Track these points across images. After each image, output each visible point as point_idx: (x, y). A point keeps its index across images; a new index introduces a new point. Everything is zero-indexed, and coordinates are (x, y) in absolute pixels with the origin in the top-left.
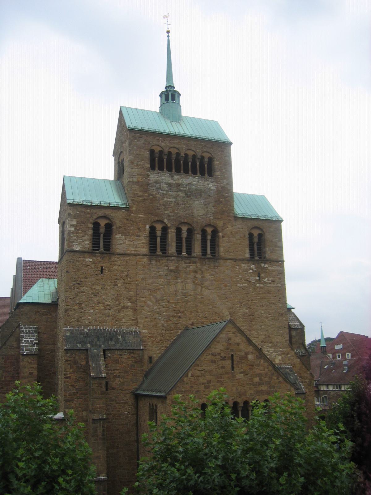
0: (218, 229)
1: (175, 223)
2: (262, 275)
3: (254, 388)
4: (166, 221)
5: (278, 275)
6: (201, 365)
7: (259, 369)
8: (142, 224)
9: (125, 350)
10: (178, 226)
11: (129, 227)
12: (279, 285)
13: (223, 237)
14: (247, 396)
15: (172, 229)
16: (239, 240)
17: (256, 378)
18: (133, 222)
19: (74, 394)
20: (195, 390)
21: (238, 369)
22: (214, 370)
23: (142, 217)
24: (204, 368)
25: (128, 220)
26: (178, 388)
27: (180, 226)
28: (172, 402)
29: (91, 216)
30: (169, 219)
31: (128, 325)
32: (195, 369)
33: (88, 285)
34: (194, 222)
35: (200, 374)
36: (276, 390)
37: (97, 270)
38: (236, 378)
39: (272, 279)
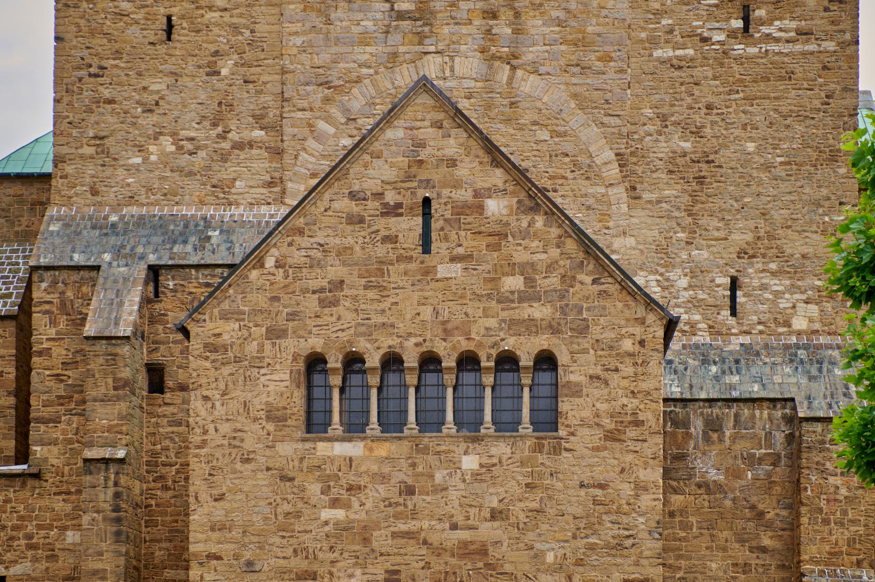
2: (760, 13)
3: (502, 309)
5: (826, 9)
6: (310, 230)
7: (525, 248)
9: (220, 270)
12: (830, 46)
14: (472, 336)
17: (511, 278)
19: (61, 401)
20: (286, 310)
26: (227, 301)
28: (206, 346)
31: (253, 201)
33: (125, 78)
35: (308, 260)
36: (584, 320)
37: (153, 27)
38: (436, 274)
39: (803, 23)
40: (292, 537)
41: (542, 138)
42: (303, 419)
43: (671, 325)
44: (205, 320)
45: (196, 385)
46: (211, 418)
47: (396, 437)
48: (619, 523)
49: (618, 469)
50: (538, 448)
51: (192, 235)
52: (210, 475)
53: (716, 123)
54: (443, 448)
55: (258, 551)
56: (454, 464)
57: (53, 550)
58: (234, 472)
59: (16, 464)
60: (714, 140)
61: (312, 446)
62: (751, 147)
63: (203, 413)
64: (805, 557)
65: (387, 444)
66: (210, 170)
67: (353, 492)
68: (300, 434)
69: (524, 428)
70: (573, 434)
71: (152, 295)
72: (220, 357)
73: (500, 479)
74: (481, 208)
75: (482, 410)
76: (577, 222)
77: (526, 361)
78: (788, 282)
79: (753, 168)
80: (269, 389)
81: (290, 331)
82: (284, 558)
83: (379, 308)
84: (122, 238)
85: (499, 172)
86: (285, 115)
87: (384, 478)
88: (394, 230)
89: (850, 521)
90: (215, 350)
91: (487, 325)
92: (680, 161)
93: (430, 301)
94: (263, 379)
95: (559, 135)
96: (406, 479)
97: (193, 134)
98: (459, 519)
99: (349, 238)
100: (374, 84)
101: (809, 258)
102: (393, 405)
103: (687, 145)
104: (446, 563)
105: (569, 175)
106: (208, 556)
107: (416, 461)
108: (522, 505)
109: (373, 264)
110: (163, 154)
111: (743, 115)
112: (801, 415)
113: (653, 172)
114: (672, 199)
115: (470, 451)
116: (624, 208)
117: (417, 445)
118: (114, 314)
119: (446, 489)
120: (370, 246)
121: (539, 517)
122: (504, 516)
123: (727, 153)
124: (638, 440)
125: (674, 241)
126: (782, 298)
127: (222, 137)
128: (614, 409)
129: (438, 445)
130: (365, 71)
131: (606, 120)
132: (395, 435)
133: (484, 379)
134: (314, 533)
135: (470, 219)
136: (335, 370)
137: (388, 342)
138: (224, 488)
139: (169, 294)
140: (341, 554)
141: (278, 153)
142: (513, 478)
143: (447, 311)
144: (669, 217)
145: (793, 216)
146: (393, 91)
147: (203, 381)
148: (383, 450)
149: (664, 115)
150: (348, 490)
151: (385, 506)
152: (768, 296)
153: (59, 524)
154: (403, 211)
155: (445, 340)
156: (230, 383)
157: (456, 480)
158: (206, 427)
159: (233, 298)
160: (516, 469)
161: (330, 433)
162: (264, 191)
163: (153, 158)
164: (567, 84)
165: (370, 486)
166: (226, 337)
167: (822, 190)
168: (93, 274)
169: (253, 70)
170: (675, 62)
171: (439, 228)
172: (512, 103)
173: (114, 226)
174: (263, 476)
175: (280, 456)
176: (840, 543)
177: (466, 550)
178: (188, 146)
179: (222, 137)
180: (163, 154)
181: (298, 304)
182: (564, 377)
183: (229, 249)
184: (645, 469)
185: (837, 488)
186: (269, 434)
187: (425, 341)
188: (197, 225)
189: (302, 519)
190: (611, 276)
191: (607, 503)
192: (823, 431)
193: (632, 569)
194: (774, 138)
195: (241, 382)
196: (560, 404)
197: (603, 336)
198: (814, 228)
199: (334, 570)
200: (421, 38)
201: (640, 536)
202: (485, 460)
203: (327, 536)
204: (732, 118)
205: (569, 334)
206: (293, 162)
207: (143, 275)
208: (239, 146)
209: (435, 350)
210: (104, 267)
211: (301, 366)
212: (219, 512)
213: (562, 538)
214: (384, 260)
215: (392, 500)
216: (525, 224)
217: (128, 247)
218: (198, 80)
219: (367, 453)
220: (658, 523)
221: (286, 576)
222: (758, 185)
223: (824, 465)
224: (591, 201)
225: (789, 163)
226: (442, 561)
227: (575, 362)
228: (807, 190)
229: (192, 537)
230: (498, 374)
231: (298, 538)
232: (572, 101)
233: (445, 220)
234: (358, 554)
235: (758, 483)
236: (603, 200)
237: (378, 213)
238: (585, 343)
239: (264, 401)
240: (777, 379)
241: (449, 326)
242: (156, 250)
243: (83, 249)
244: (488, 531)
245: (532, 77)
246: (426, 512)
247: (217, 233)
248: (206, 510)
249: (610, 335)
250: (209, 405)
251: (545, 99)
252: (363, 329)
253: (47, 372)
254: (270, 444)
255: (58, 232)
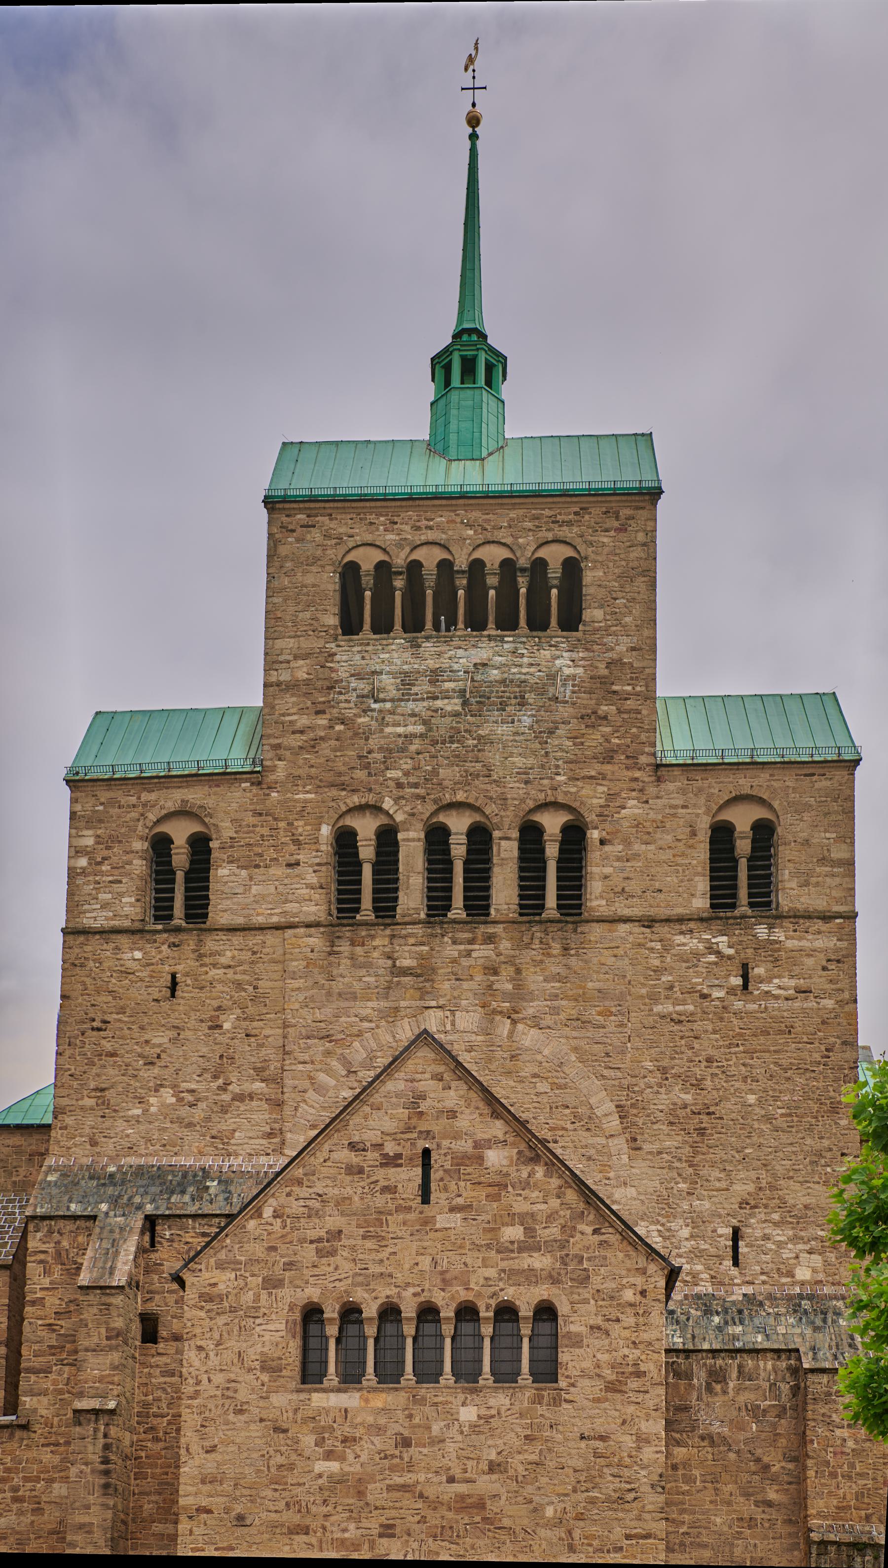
0: (586, 815)
1: (419, 807)
3: (502, 1259)
4: (388, 804)
7: (525, 1198)
8: (306, 825)
9: (217, 1220)
10: (435, 820)
11: (262, 836)
13: (602, 842)
15: (408, 830)
16: (670, 847)
18: (275, 819)
19: (53, 1351)
20: (283, 1260)
21: (444, 1195)
22: (356, 1198)
23: (306, 801)
24: (321, 1192)
25: (260, 814)
26: (224, 1250)
27: (442, 818)
29: (142, 815)
30: (403, 797)
32: (288, 1195)
34: (491, 798)
35: (306, 1210)
36: (585, 1270)
38: (435, 1224)
40: (284, 1490)
41: (542, 1090)
42: (298, 1369)
43: (673, 1275)
44: (200, 1270)
45: (190, 1335)
46: (204, 1369)
47: (392, 1388)
48: (620, 1477)
49: (619, 1421)
50: (538, 1400)
51: (190, 1185)
52: (202, 1426)
53: (717, 1075)
54: (440, 1399)
55: (249, 1505)
56: (452, 1415)
57: (39, 1503)
58: (227, 1423)
59: (4, 1415)
60: (714, 1092)
61: (308, 1397)
62: (752, 1099)
63: (197, 1363)
64: (812, 1511)
65: (384, 1395)
66: (210, 1121)
67: (348, 1444)
68: (293, 1385)
69: (523, 1379)
70: (573, 1385)
71: (147, 1245)
72: (215, 1307)
73: (499, 1430)
74: (480, 1159)
75: (481, 1361)
76: (578, 1173)
77: (526, 1311)
78: (791, 1233)
79: (754, 1120)
80: (264, 1339)
81: (286, 1281)
82: (276, 1511)
83: (377, 1258)
84: (119, 1188)
85: (499, 1123)
86: (286, 1068)
87: (379, 1430)
88: (393, 1180)
89: (857, 1474)
90: (211, 1300)
91: (487, 1275)
92: (681, 1113)
93: (429, 1251)
94: (258, 1329)
95: (559, 1087)
96: (402, 1430)
97: (193, 1086)
98: (457, 1472)
99: (348, 1188)
100: (375, 1038)
101: (811, 1209)
102: (389, 1356)
103: (688, 1098)
104: (443, 1517)
105: (569, 1126)
106: (197, 1510)
107: (412, 1412)
108: (521, 1457)
109: (371, 1215)
110: (163, 1105)
111: (743, 1068)
112: (806, 1366)
113: (653, 1123)
114: (673, 1150)
115: (468, 1402)
116: (625, 1158)
117: (414, 1396)
118: (109, 1264)
119: (443, 1441)
120: (369, 1196)
121: (538, 1470)
122: (502, 1469)
123: (729, 1105)
124: (639, 1391)
125: (675, 1192)
126: (784, 1248)
127: (223, 1088)
128: (615, 1360)
129: (435, 1396)
130: (366, 1025)
131: (606, 1072)
132: (391, 1386)
133: (483, 1330)
134: (307, 1486)
135: (469, 1170)
136: (331, 1320)
137: (385, 1292)
138: (216, 1440)
139: (166, 1244)
140: (335, 1508)
141: (279, 1104)
142: (512, 1430)
143: (445, 1261)
144: (670, 1168)
145: (794, 1167)
146: (394, 1044)
147: (198, 1331)
148: (379, 1400)
149: (664, 1068)
150: (342, 1442)
151: (381, 1459)
152: (770, 1245)
153: (46, 1476)
154: (403, 1161)
155: (443, 1290)
156: (224, 1333)
157: (454, 1432)
158: (199, 1378)
159: (229, 1248)
160: (514, 1421)
161: (326, 1384)
162: (264, 1142)
163: (153, 1109)
164: (567, 1037)
165: (365, 1437)
166: (221, 1286)
167: (823, 1141)
168: (90, 1224)
169: (255, 1024)
170: (675, 1016)
171: (438, 1178)
172: (513, 1057)
173: (112, 1176)
174: (256, 1428)
175: (274, 1407)
176: (848, 1497)
177: (462, 1504)
178: (189, 1098)
179: (223, 1088)
180: (163, 1105)
181: (295, 1254)
182: (563, 1329)
183: (226, 1199)
184: (647, 1420)
185: (845, 1440)
186: (263, 1385)
187: (423, 1291)
188: (195, 1176)
189: (295, 1471)
190: (612, 1226)
191: (608, 1455)
192: (828, 1382)
193: (634, 1523)
194: (774, 1090)
195: (235, 1332)
196: (560, 1355)
197: (603, 1287)
198: (816, 1179)
199: (327, 1524)
200: (423, 994)
201: (642, 1490)
202: (483, 1412)
203: (321, 1489)
204: (733, 1070)
205: (570, 1284)
206: (293, 1113)
207: (139, 1224)
208: (240, 1098)
209: (433, 1300)
210: (101, 1216)
211: (297, 1316)
212: (210, 1464)
213: (561, 1491)
214: (383, 1210)
215: (388, 1452)
216: (525, 1175)
217: (126, 1197)
218: (200, 1033)
219: (363, 1404)
220: (661, 1476)
221: (278, 1531)
222: (759, 1137)
223: (830, 1417)
224: (592, 1152)
225: (790, 1115)
226: (438, 1515)
227: (575, 1312)
228: (809, 1141)
229: (182, 1488)
230: (497, 1324)
231: (290, 1491)
232: (573, 1055)
233: (445, 1171)
234: (352, 1507)
235: (763, 1436)
236: (603, 1151)
237: (378, 1163)
238: (586, 1294)
239: (259, 1351)
240: (781, 1330)
241: (448, 1276)
242: (153, 1201)
243: (80, 1199)
244: (486, 1484)
245: (533, 1031)
246: (423, 1465)
247: (215, 1183)
248: (197, 1462)
249: (611, 1285)
250: (203, 1355)
251: (546, 1052)
252: (360, 1279)
253: (40, 1322)
254: (264, 1395)
255: (56, 1182)
